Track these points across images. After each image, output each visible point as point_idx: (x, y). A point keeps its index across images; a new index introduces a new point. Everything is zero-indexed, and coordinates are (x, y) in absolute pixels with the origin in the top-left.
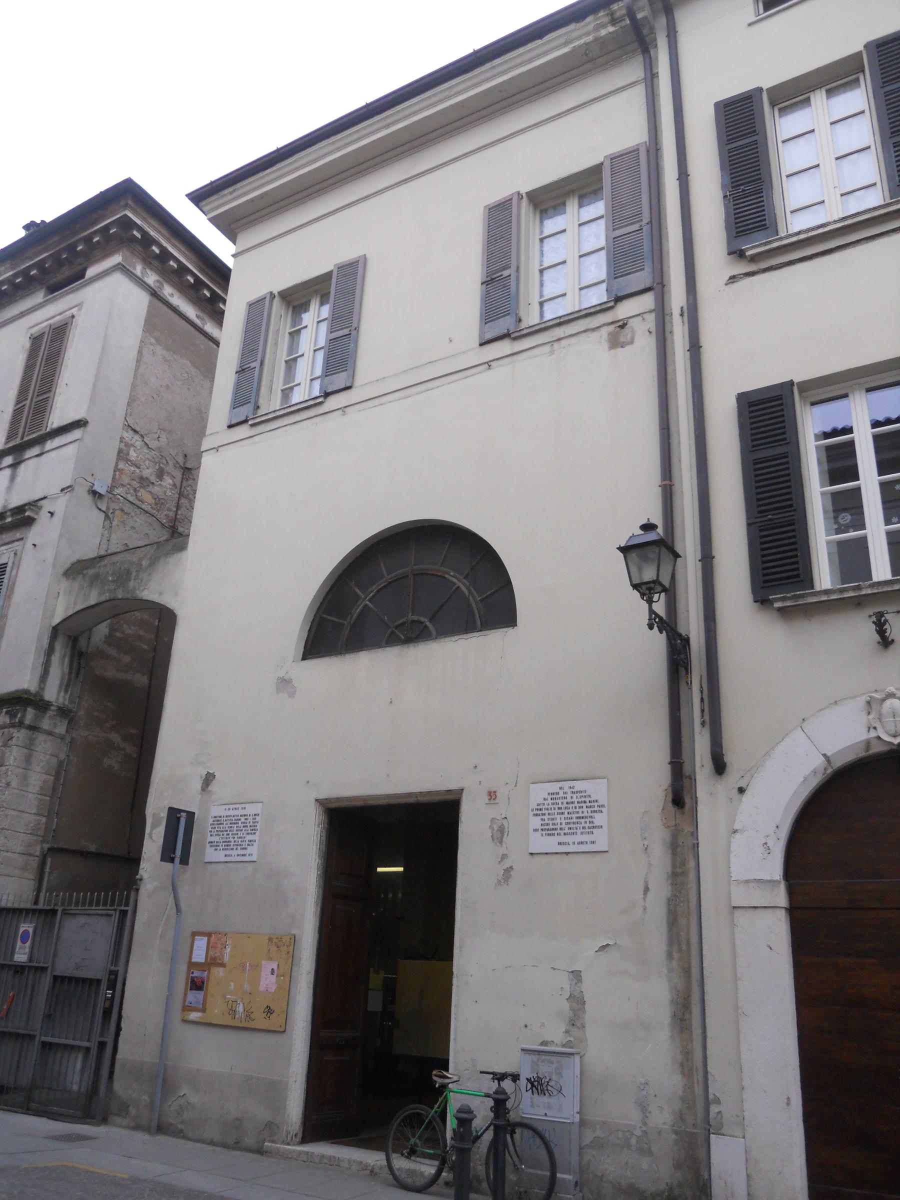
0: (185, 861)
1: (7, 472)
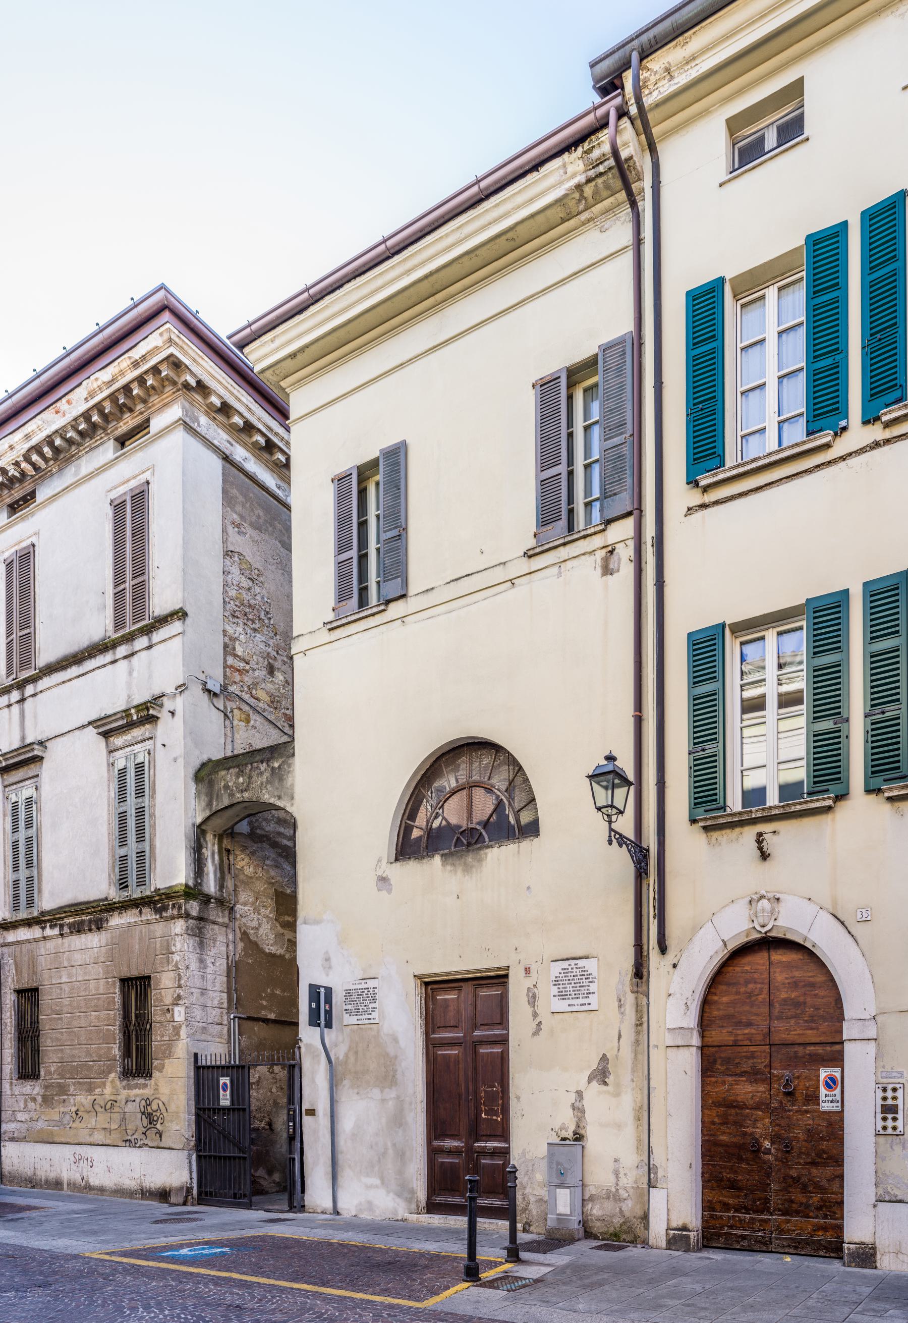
0: (329, 1025)
1: (16, 709)
